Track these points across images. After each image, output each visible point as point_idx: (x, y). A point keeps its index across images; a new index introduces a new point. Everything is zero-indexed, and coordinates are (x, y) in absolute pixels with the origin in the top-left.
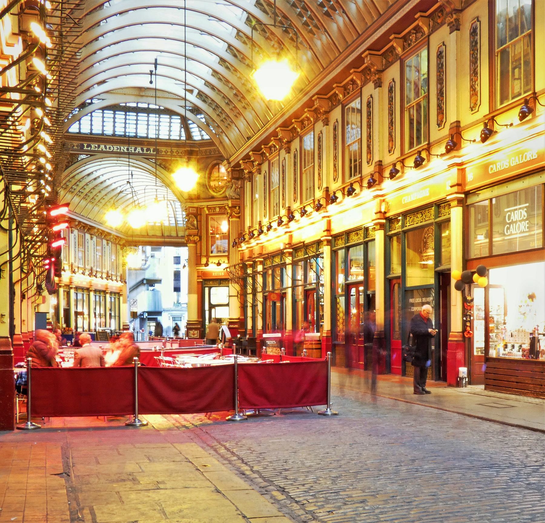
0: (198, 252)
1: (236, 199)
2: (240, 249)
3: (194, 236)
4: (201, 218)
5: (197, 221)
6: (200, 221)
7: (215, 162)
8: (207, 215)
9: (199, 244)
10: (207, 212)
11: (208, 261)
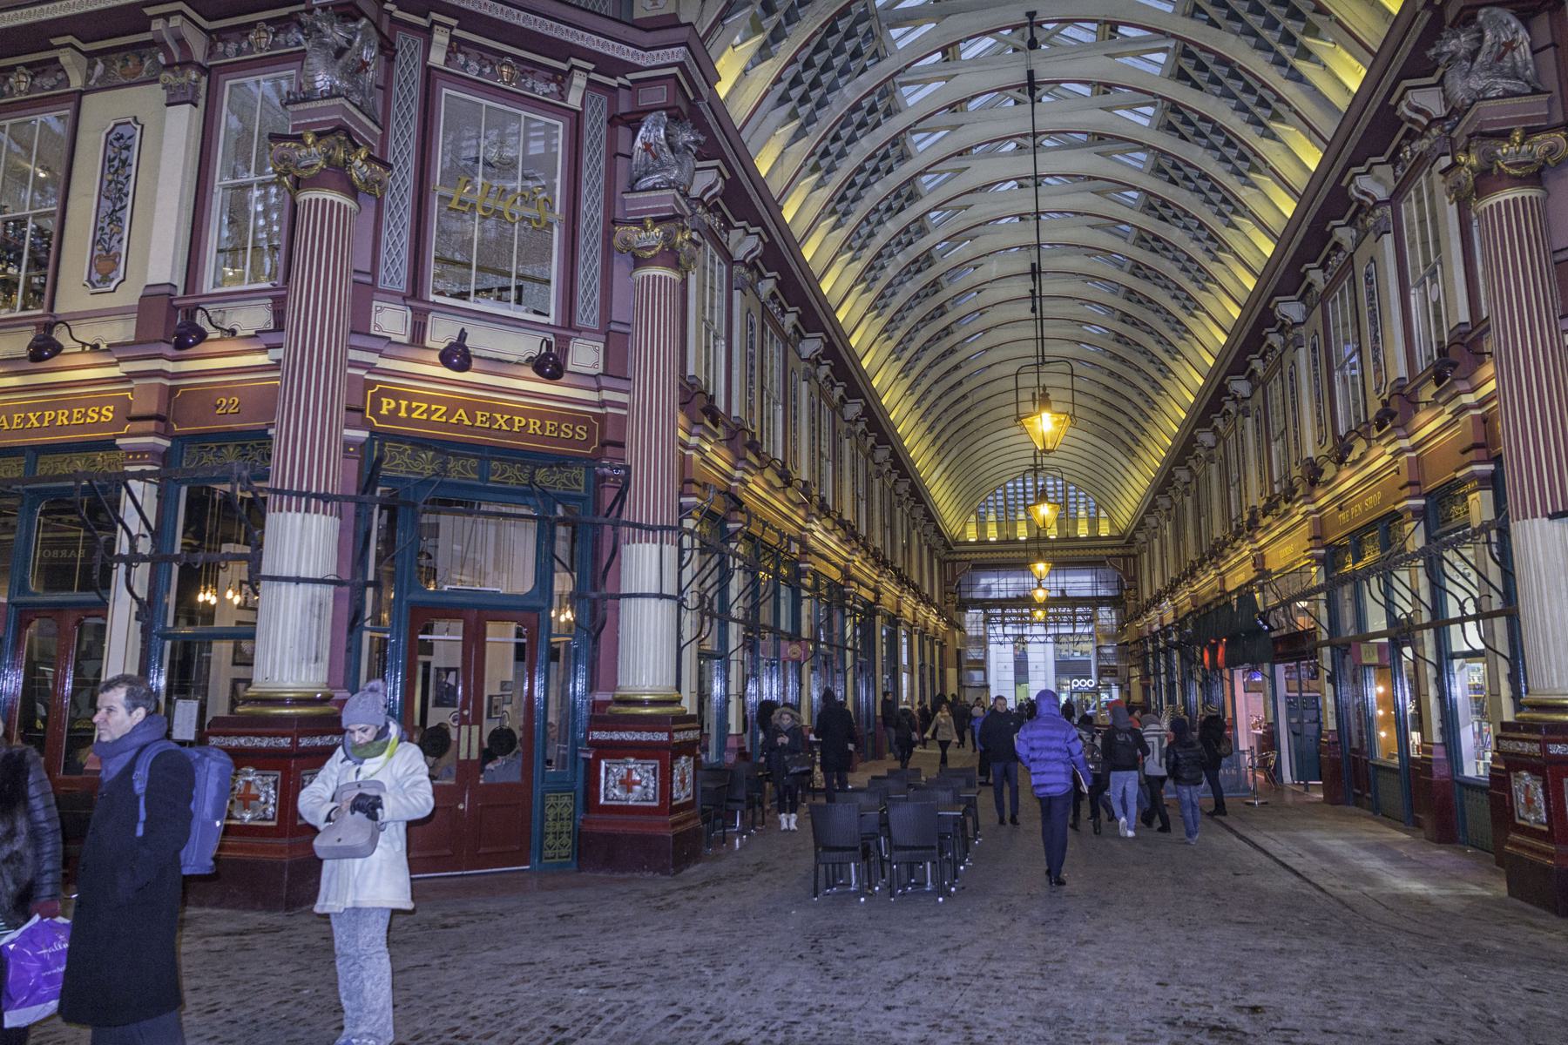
3: (1529, 133)
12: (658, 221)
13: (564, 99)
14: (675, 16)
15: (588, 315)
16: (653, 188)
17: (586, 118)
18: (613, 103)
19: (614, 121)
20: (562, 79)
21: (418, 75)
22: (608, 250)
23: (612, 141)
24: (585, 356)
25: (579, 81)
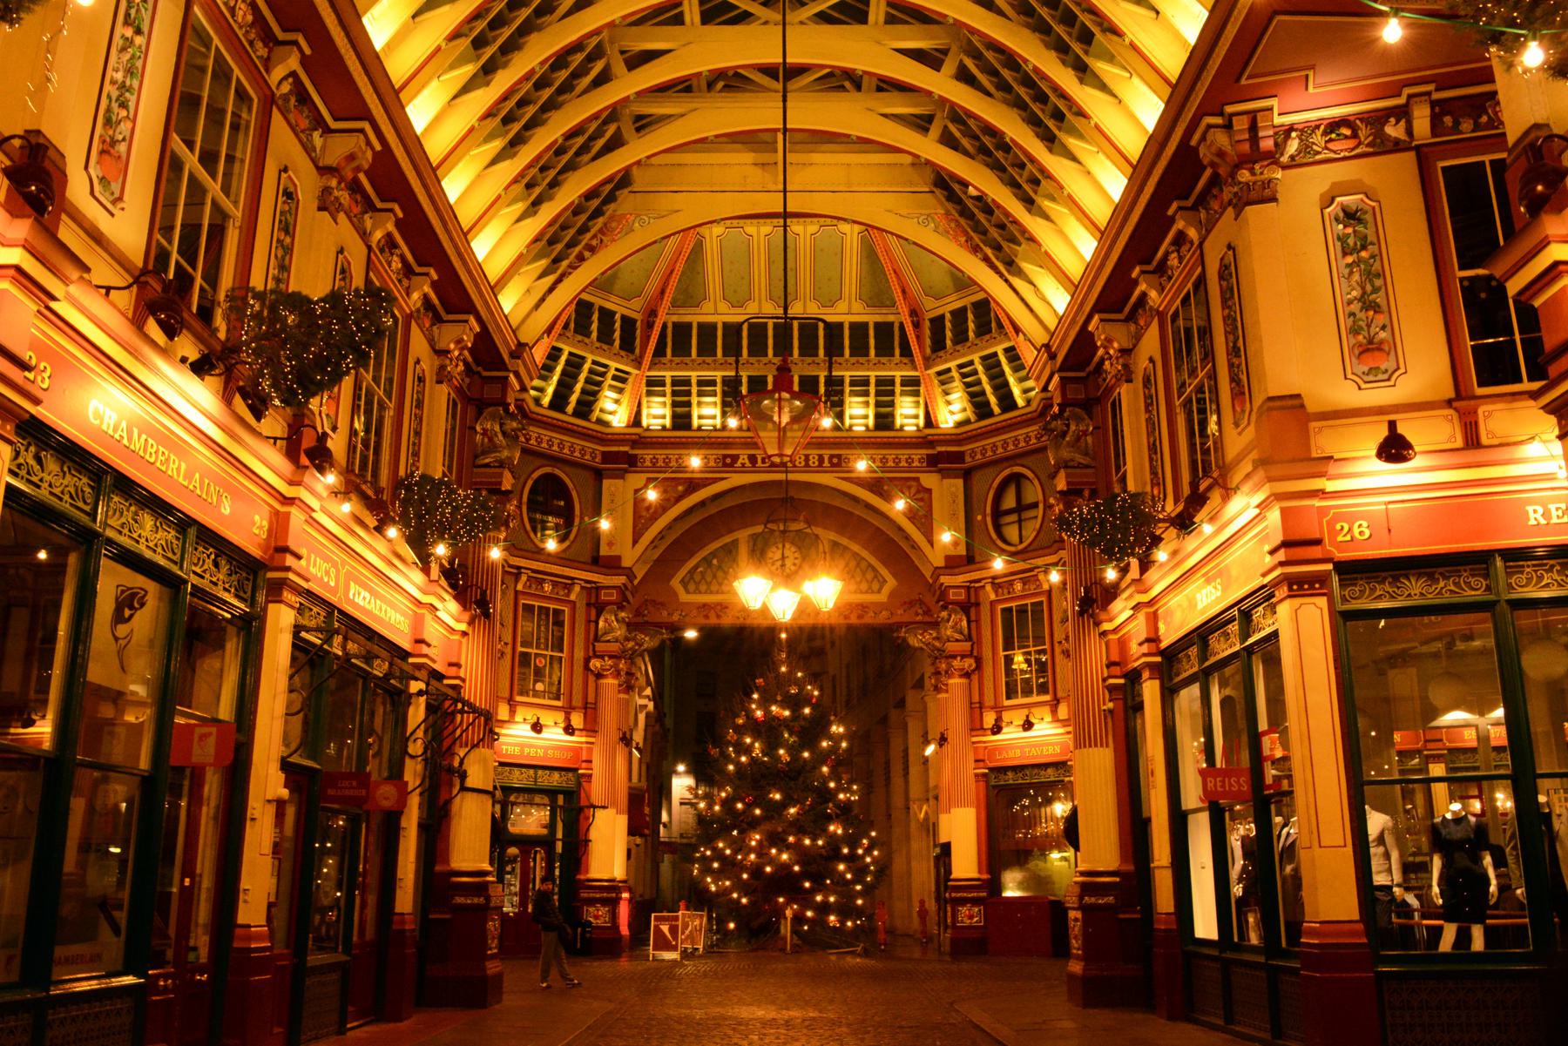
0: (976, 699)
1: (1080, 466)
2: (1106, 626)
3: (963, 657)
4: (978, 614)
5: (969, 622)
6: (978, 621)
7: (1007, 472)
8: (992, 603)
9: (975, 677)
10: (993, 597)
11: (999, 719)
12: (611, 657)
13: (568, 595)
14: (618, 558)
15: (577, 700)
16: (608, 641)
17: (578, 605)
18: (589, 594)
19: (588, 605)
20: (568, 588)
21: (512, 596)
22: (586, 667)
23: (588, 614)
24: (577, 720)
25: (577, 588)
